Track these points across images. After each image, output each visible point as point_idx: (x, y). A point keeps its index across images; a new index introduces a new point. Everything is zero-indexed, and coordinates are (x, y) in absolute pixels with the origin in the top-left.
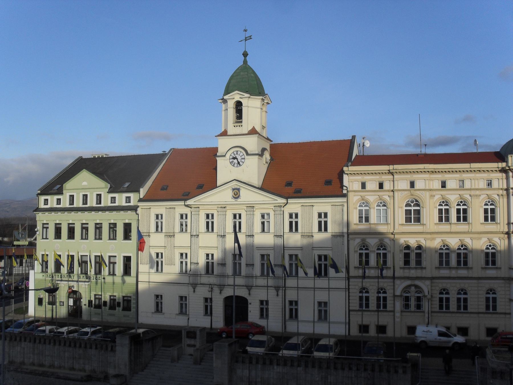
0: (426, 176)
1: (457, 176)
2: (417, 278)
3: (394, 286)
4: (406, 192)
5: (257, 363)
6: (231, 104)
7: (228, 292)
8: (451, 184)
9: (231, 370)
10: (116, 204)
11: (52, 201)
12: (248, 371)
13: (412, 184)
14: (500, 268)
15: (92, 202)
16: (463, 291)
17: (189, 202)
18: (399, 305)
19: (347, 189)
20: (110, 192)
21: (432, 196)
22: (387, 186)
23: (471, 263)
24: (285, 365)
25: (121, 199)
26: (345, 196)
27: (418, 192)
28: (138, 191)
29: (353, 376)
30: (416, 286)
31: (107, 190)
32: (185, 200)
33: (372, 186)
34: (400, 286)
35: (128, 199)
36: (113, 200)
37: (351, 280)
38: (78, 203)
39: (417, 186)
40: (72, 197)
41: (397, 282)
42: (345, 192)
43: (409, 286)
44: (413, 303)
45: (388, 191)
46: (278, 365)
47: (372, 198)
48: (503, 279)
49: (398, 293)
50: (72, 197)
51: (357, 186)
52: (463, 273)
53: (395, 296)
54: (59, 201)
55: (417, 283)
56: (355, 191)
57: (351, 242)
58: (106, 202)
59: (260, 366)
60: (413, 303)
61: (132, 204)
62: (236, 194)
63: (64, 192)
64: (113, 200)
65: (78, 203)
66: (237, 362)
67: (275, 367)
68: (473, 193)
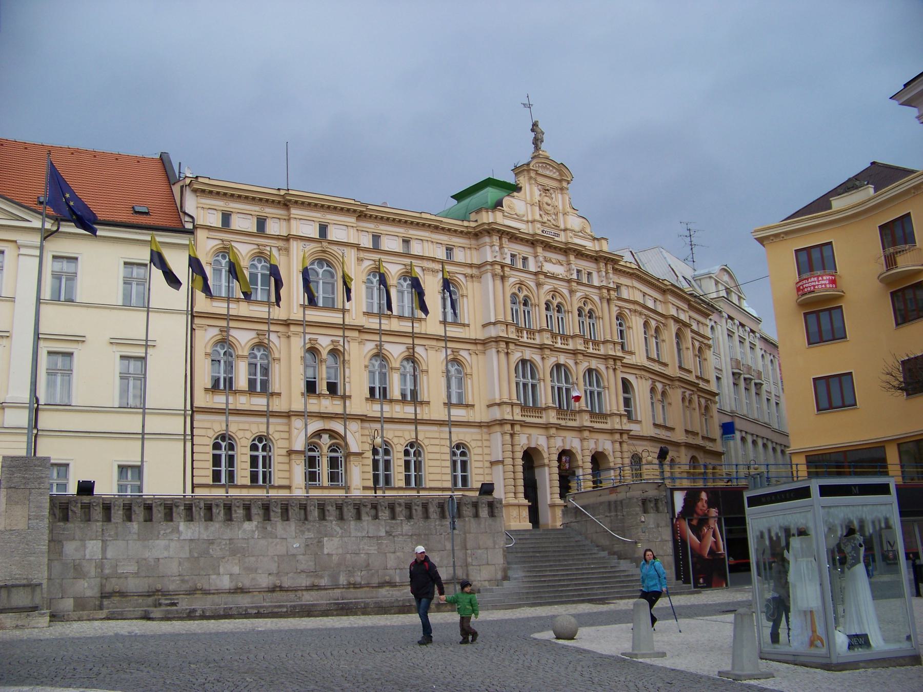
0: (352, 220)
1: (401, 231)
3: (289, 432)
4: (313, 245)
5: (129, 518)
9: (55, 542)
12: (100, 543)
13: (323, 229)
14: (473, 406)
18: (299, 470)
19: (193, 222)
21: (360, 260)
22: (273, 228)
23: (426, 395)
24: (209, 518)
26: (191, 232)
27: (335, 248)
29: (383, 533)
30: (333, 434)
33: (243, 223)
37: (197, 417)
39: (335, 233)
41: (297, 423)
42: (189, 226)
43: (318, 434)
44: (324, 469)
45: (278, 238)
46: (190, 518)
48: (480, 425)
51: (215, 220)
53: (290, 453)
55: (338, 426)
56: (210, 228)
57: (198, 333)
59: (134, 526)
60: (324, 469)
66: (66, 519)
67: (182, 526)
68: (426, 264)
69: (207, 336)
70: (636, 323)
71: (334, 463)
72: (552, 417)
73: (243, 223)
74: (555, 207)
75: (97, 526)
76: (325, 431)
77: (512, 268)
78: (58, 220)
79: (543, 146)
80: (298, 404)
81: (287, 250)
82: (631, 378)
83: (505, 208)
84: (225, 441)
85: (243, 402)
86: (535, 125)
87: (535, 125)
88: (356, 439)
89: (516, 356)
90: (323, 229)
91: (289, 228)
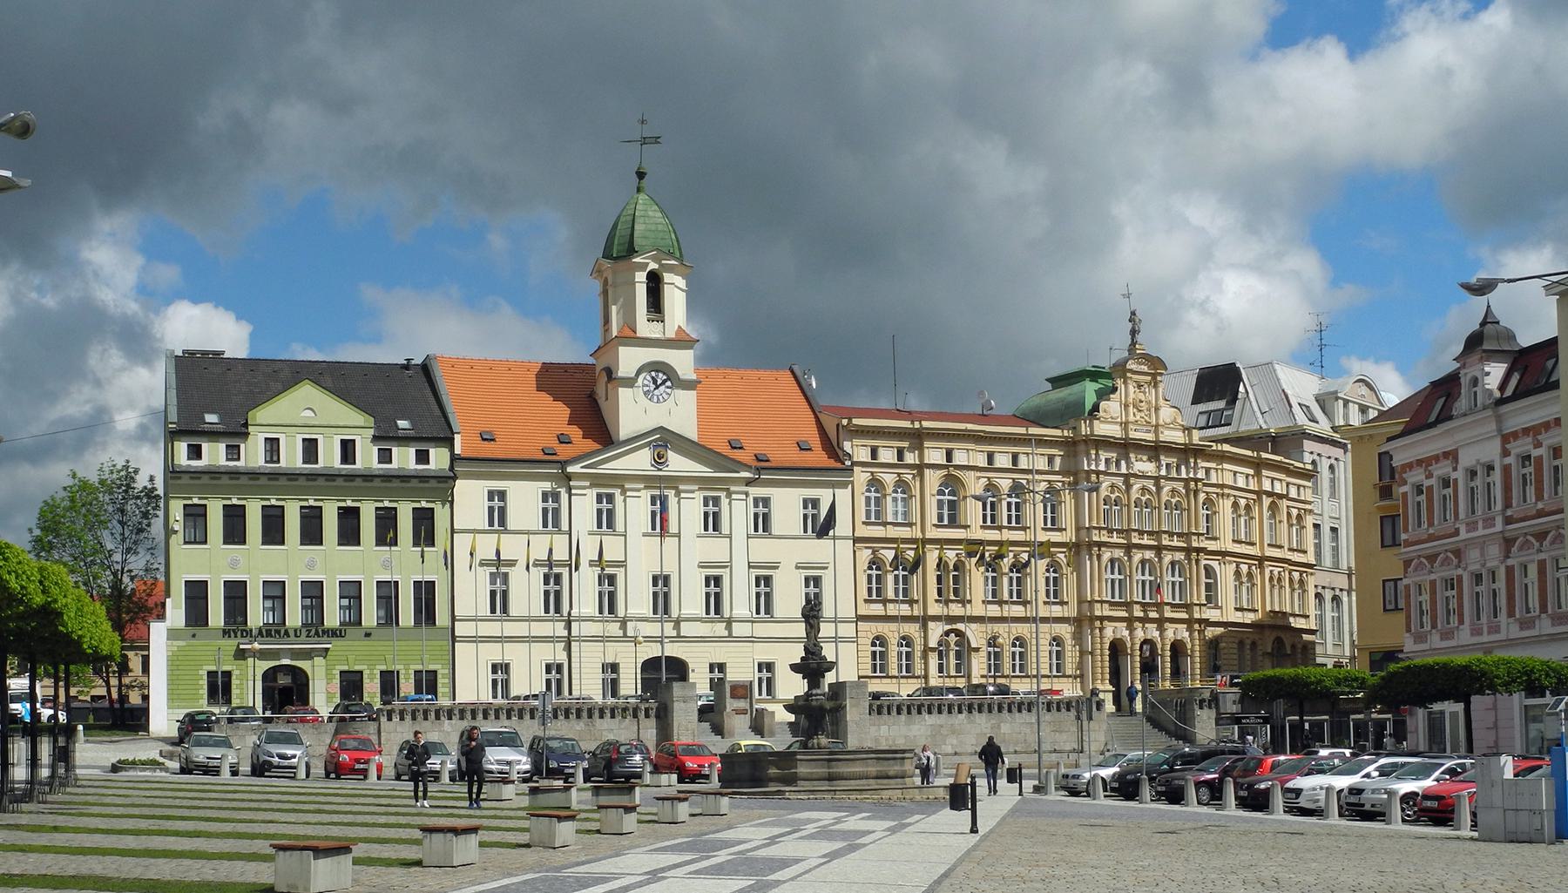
2: (960, 619)
6: (641, 277)
7: (653, 651)
8: (1003, 461)
10: (394, 465)
11: (214, 454)
13: (949, 455)
15: (329, 456)
16: (1020, 641)
17: (570, 469)
20: (375, 439)
22: (910, 458)
25: (404, 458)
28: (448, 441)
30: (959, 633)
31: (372, 432)
32: (563, 464)
34: (936, 631)
35: (423, 457)
36: (385, 456)
38: (290, 457)
39: (960, 458)
40: (273, 445)
41: (931, 625)
42: (848, 463)
43: (947, 633)
47: (889, 478)
49: (933, 643)
50: (273, 445)
51: (863, 455)
52: (1018, 611)
54: (233, 452)
58: (367, 457)
61: (432, 466)
62: (659, 460)
63: (251, 429)
64: (385, 456)
65: (290, 457)
69: (865, 555)
70: (1225, 506)
71: (958, 655)
72: (1138, 613)
73: (887, 455)
74: (1149, 403)
75: (903, 717)
76: (952, 631)
77: (1105, 473)
78: (759, 470)
79: (1139, 338)
80: (935, 609)
81: (921, 475)
82: (1215, 564)
83: (1101, 414)
84: (880, 640)
85: (892, 610)
86: (1133, 313)
87: (1133, 313)
88: (976, 635)
89: (1106, 556)
90: (949, 455)
91: (921, 456)
